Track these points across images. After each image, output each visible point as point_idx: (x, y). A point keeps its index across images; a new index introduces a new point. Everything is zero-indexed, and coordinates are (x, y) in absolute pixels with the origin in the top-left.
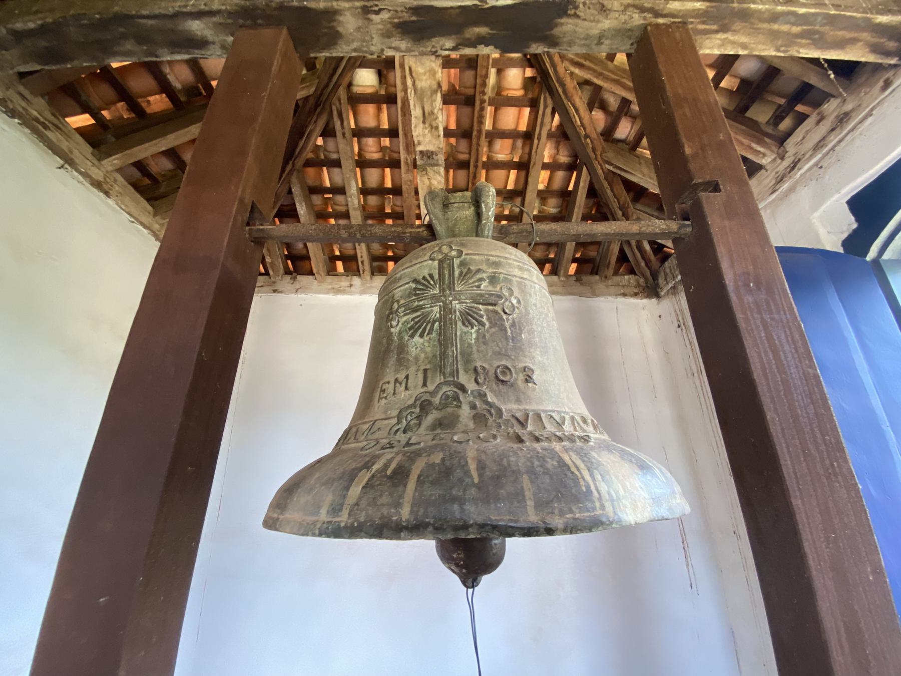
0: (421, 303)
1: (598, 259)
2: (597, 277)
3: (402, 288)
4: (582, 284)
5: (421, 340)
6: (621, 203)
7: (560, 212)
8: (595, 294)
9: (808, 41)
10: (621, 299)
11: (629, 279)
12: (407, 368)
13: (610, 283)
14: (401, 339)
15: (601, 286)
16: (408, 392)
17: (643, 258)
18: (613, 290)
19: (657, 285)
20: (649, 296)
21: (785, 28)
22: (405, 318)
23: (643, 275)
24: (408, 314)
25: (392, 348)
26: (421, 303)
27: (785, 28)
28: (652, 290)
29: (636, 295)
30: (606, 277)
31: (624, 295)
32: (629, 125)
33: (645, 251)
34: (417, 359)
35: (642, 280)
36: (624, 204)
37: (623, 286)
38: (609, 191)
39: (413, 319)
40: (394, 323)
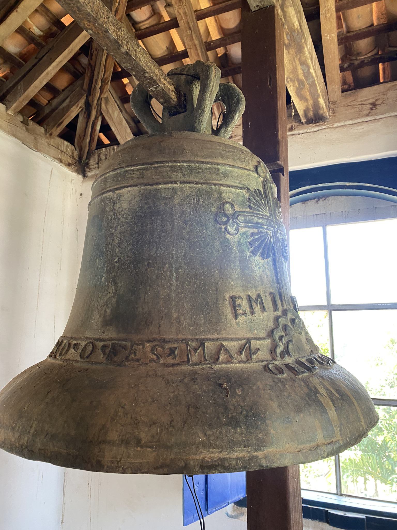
0: (260, 221)
1: (47, 111)
2: (42, 130)
3: (233, 190)
4: (27, 129)
5: (262, 261)
6: (105, 76)
7: (40, 36)
8: (37, 148)
9: (298, 86)
10: (56, 164)
11: (67, 146)
12: (256, 287)
13: (52, 141)
14: (242, 251)
15: (43, 141)
16: (266, 313)
17: (91, 136)
18: (53, 151)
19: (87, 164)
20: (78, 172)
21: (300, 71)
22: (243, 230)
23: (81, 149)
24: (249, 227)
25: (232, 258)
26: (260, 221)
27: (300, 71)
28: (81, 166)
29: (69, 165)
30: (51, 135)
31: (61, 161)
32: (148, 15)
33: (95, 130)
34: (261, 279)
35: (76, 153)
36: (106, 79)
37: (62, 151)
38: (104, 59)
39: (252, 235)
40: (231, 229)
